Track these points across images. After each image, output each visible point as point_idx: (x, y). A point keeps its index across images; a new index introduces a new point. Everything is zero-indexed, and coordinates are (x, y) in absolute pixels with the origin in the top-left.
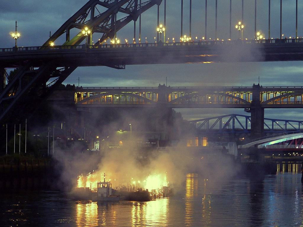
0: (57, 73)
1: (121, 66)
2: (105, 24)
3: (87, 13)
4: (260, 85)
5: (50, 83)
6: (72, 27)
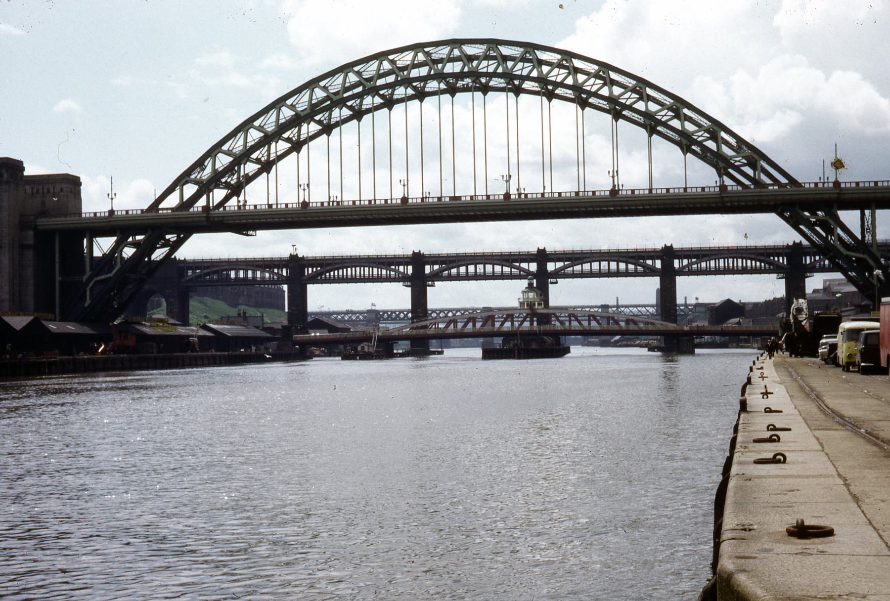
0: (167, 243)
1: (251, 233)
2: (230, 179)
3: (206, 164)
4: (422, 252)
5: (159, 254)
6: (187, 182)
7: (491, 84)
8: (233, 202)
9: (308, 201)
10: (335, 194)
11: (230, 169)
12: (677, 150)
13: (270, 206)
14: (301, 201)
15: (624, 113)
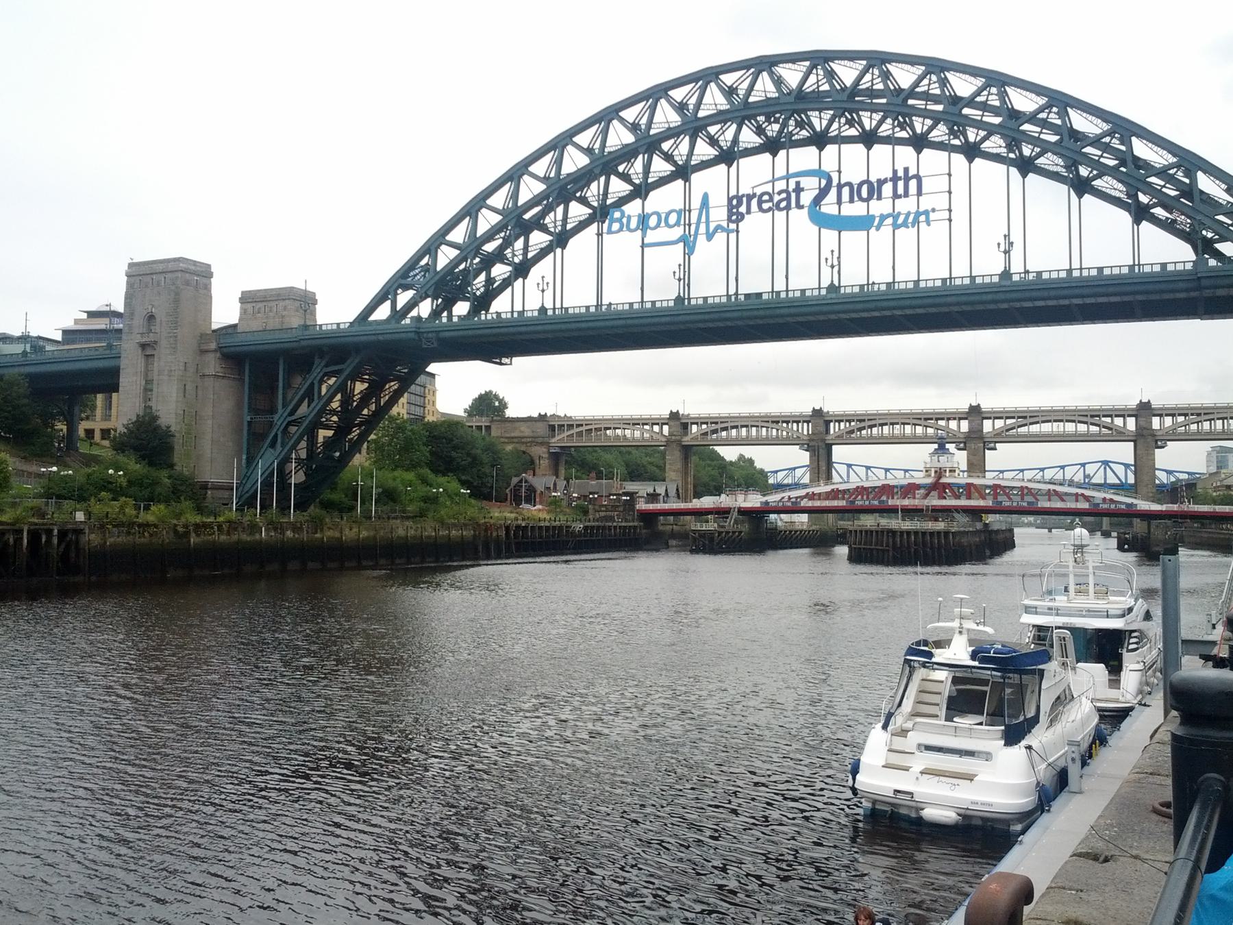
10: (780, 286)
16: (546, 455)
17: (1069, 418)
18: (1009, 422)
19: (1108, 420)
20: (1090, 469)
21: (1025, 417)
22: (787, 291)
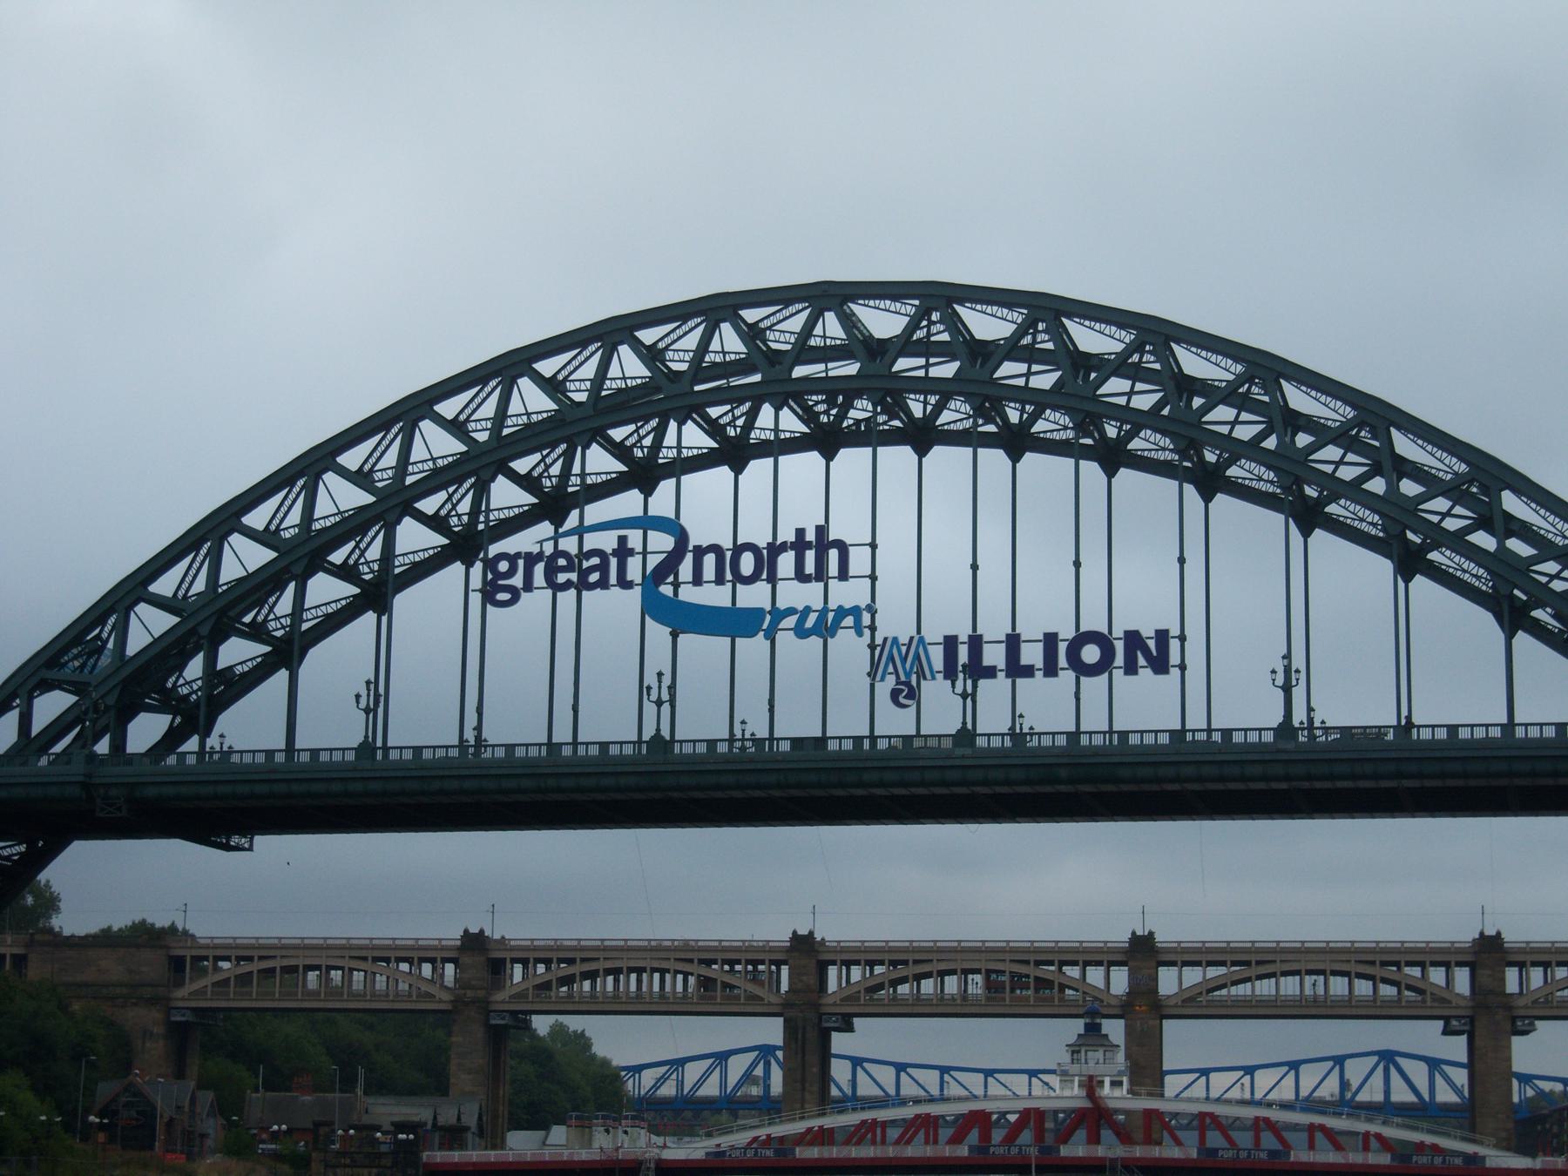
7: (1136, 444)
8: (192, 744)
9: (668, 738)
11: (170, 652)
12: (1488, 618)
13: (552, 747)
14: (646, 737)
15: (1332, 509)
16: (159, 1030)
17: (1337, 967)
18: (1213, 972)
19: (1416, 972)
20: (1355, 1071)
21: (1247, 963)
22: (575, 743)
